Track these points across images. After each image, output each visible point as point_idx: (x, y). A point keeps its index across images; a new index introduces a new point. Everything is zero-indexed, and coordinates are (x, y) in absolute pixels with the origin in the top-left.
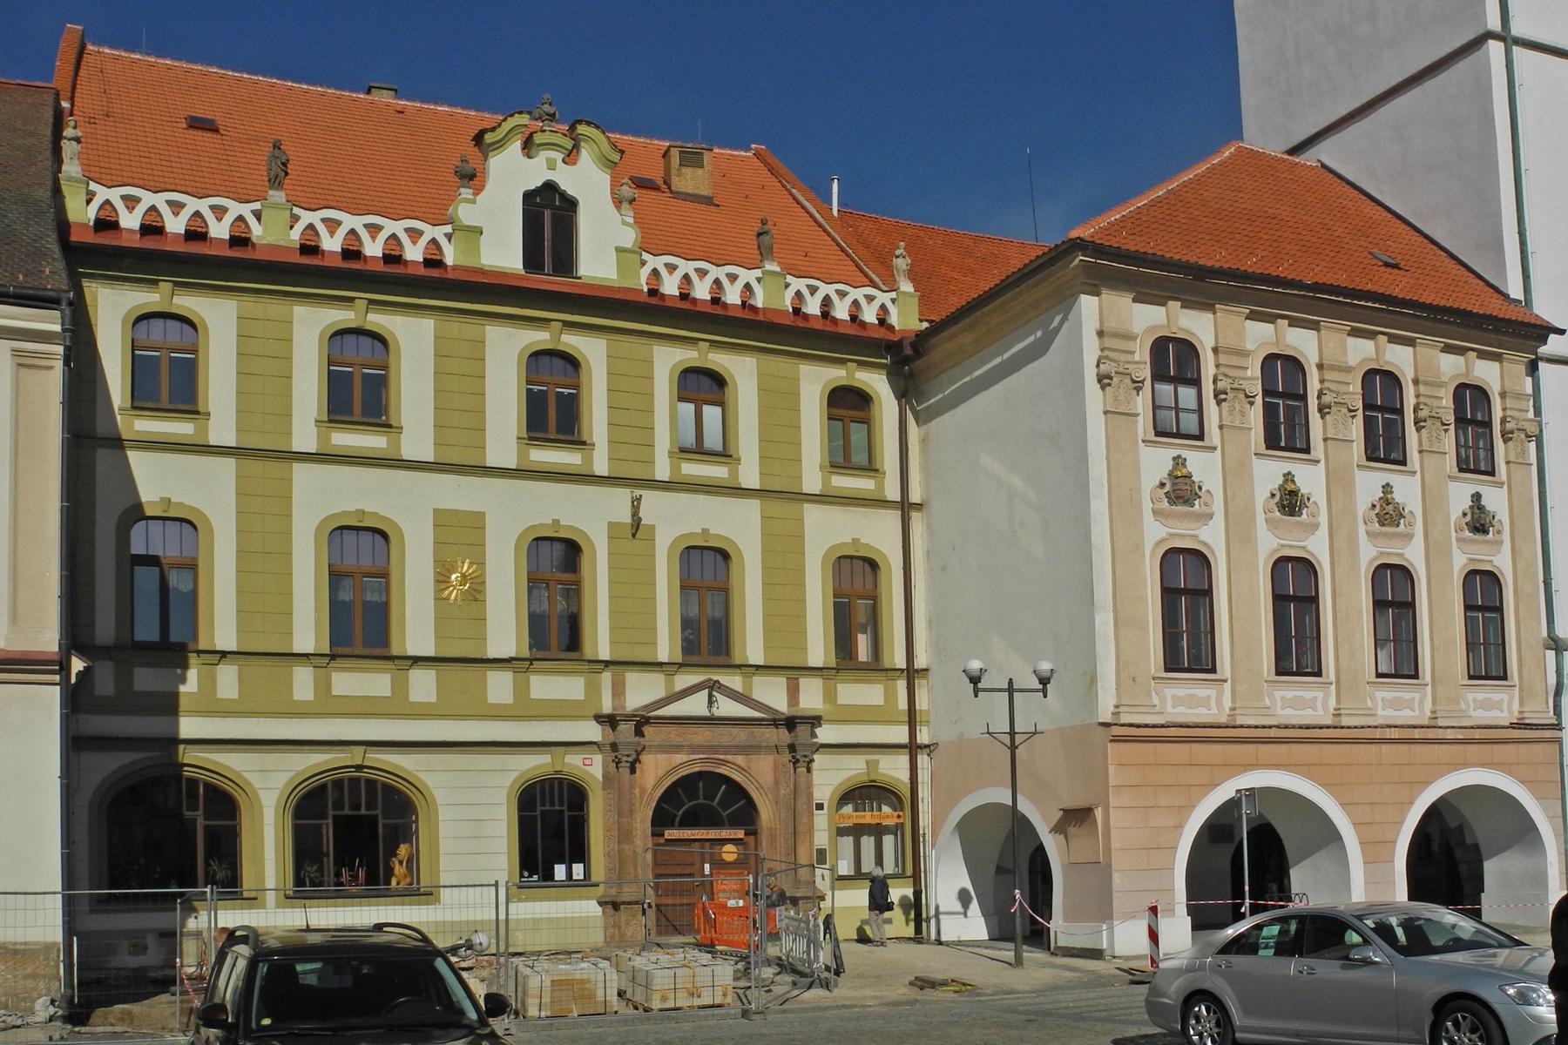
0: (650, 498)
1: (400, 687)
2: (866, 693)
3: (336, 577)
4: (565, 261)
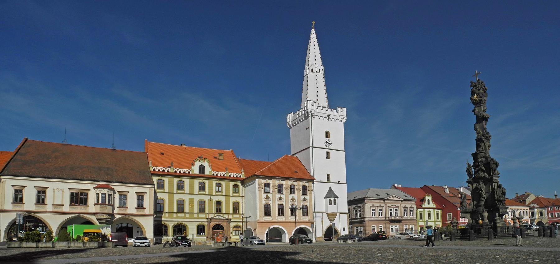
0: (212, 197)
1: (185, 216)
2: (237, 216)
3: (178, 205)
4: (203, 172)
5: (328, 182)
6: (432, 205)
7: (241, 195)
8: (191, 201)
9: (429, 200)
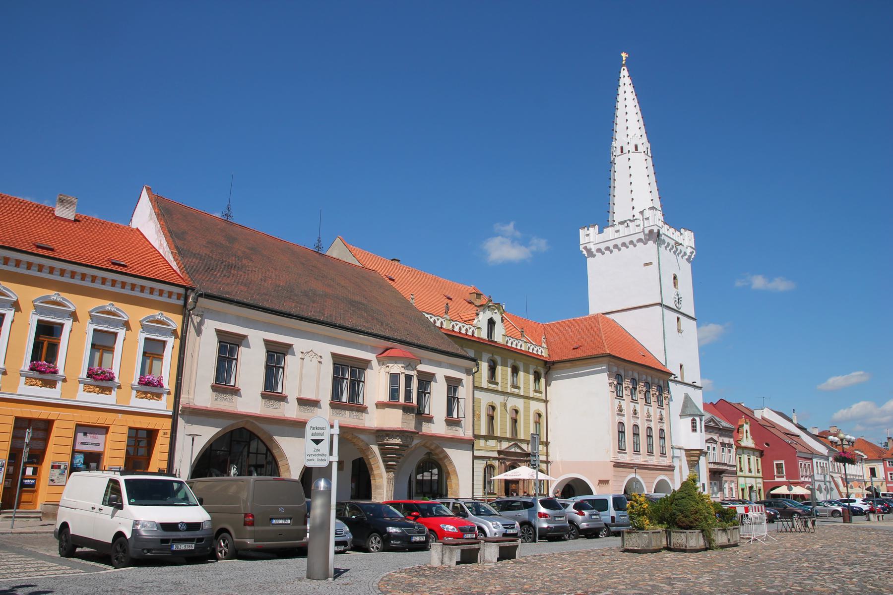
9: (747, 431)
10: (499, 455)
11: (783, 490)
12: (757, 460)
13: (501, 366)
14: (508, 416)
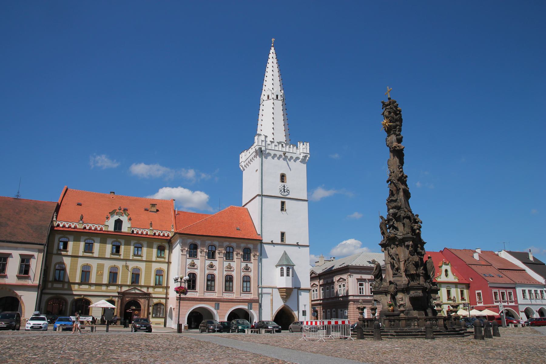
5: (282, 243)
6: (452, 278)
7: (167, 260)
8: (100, 267)
9: (446, 271)
10: (119, 295)
11: (461, 312)
12: (462, 292)
13: (125, 245)
14: (129, 273)
